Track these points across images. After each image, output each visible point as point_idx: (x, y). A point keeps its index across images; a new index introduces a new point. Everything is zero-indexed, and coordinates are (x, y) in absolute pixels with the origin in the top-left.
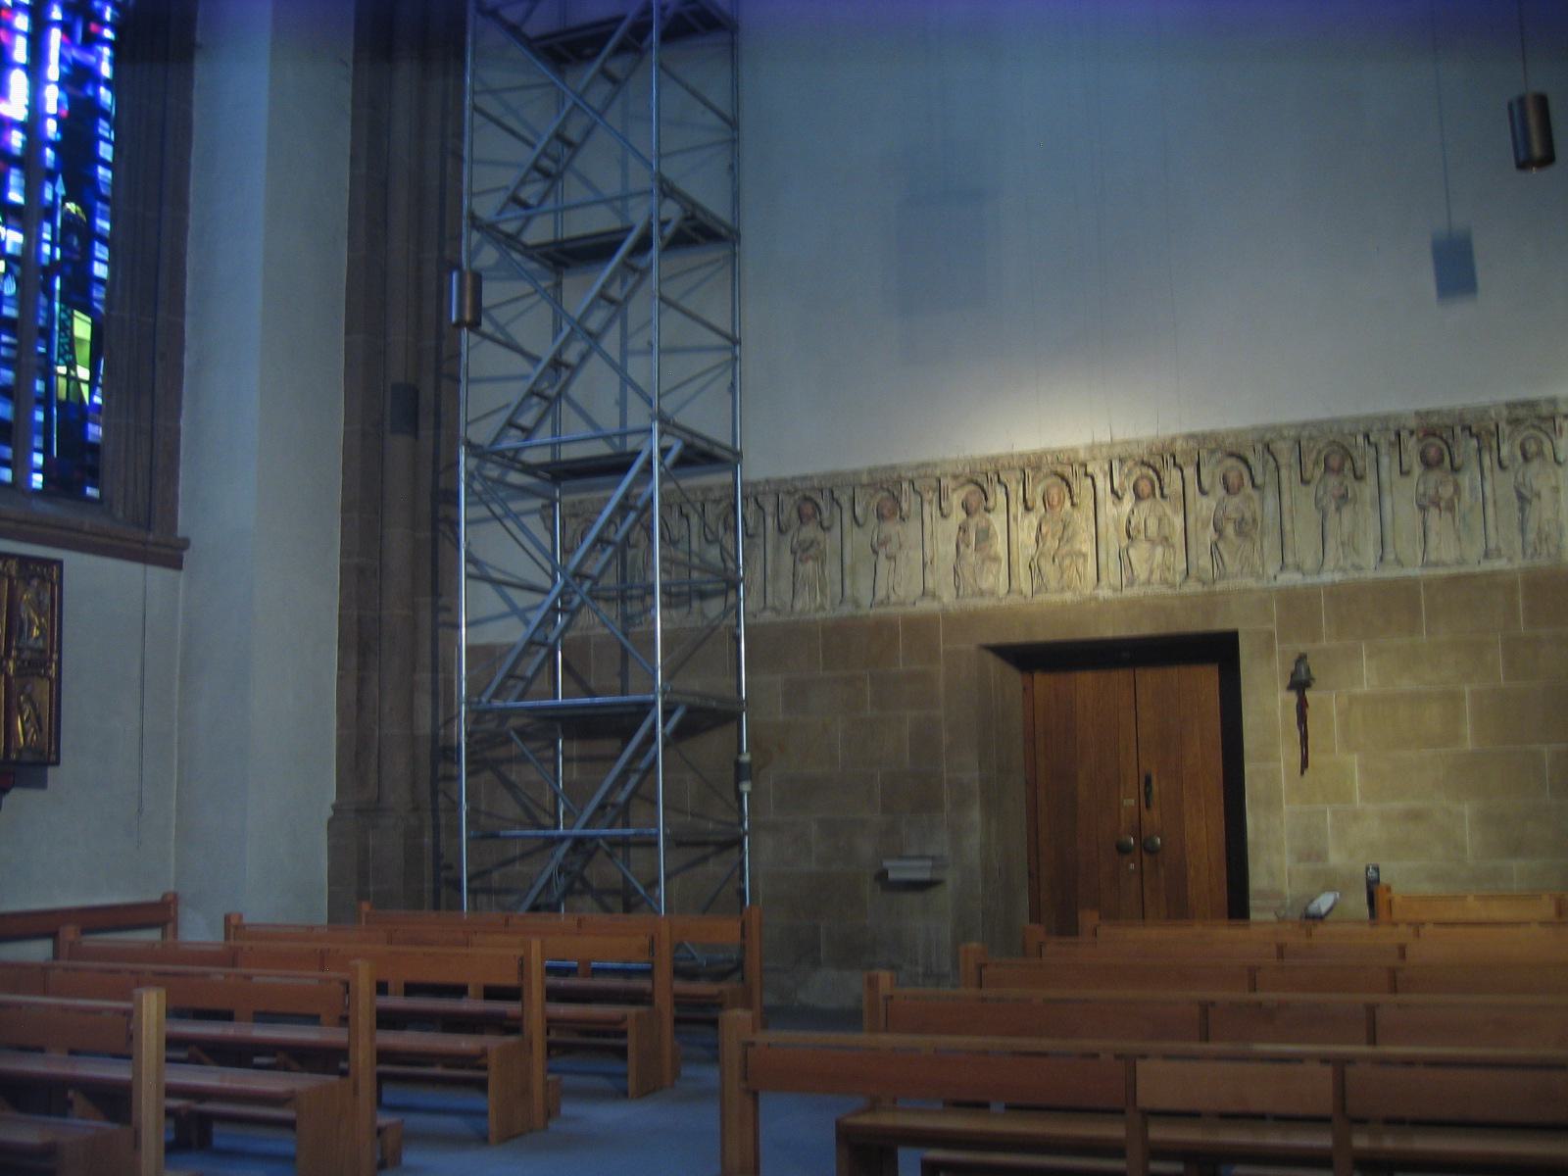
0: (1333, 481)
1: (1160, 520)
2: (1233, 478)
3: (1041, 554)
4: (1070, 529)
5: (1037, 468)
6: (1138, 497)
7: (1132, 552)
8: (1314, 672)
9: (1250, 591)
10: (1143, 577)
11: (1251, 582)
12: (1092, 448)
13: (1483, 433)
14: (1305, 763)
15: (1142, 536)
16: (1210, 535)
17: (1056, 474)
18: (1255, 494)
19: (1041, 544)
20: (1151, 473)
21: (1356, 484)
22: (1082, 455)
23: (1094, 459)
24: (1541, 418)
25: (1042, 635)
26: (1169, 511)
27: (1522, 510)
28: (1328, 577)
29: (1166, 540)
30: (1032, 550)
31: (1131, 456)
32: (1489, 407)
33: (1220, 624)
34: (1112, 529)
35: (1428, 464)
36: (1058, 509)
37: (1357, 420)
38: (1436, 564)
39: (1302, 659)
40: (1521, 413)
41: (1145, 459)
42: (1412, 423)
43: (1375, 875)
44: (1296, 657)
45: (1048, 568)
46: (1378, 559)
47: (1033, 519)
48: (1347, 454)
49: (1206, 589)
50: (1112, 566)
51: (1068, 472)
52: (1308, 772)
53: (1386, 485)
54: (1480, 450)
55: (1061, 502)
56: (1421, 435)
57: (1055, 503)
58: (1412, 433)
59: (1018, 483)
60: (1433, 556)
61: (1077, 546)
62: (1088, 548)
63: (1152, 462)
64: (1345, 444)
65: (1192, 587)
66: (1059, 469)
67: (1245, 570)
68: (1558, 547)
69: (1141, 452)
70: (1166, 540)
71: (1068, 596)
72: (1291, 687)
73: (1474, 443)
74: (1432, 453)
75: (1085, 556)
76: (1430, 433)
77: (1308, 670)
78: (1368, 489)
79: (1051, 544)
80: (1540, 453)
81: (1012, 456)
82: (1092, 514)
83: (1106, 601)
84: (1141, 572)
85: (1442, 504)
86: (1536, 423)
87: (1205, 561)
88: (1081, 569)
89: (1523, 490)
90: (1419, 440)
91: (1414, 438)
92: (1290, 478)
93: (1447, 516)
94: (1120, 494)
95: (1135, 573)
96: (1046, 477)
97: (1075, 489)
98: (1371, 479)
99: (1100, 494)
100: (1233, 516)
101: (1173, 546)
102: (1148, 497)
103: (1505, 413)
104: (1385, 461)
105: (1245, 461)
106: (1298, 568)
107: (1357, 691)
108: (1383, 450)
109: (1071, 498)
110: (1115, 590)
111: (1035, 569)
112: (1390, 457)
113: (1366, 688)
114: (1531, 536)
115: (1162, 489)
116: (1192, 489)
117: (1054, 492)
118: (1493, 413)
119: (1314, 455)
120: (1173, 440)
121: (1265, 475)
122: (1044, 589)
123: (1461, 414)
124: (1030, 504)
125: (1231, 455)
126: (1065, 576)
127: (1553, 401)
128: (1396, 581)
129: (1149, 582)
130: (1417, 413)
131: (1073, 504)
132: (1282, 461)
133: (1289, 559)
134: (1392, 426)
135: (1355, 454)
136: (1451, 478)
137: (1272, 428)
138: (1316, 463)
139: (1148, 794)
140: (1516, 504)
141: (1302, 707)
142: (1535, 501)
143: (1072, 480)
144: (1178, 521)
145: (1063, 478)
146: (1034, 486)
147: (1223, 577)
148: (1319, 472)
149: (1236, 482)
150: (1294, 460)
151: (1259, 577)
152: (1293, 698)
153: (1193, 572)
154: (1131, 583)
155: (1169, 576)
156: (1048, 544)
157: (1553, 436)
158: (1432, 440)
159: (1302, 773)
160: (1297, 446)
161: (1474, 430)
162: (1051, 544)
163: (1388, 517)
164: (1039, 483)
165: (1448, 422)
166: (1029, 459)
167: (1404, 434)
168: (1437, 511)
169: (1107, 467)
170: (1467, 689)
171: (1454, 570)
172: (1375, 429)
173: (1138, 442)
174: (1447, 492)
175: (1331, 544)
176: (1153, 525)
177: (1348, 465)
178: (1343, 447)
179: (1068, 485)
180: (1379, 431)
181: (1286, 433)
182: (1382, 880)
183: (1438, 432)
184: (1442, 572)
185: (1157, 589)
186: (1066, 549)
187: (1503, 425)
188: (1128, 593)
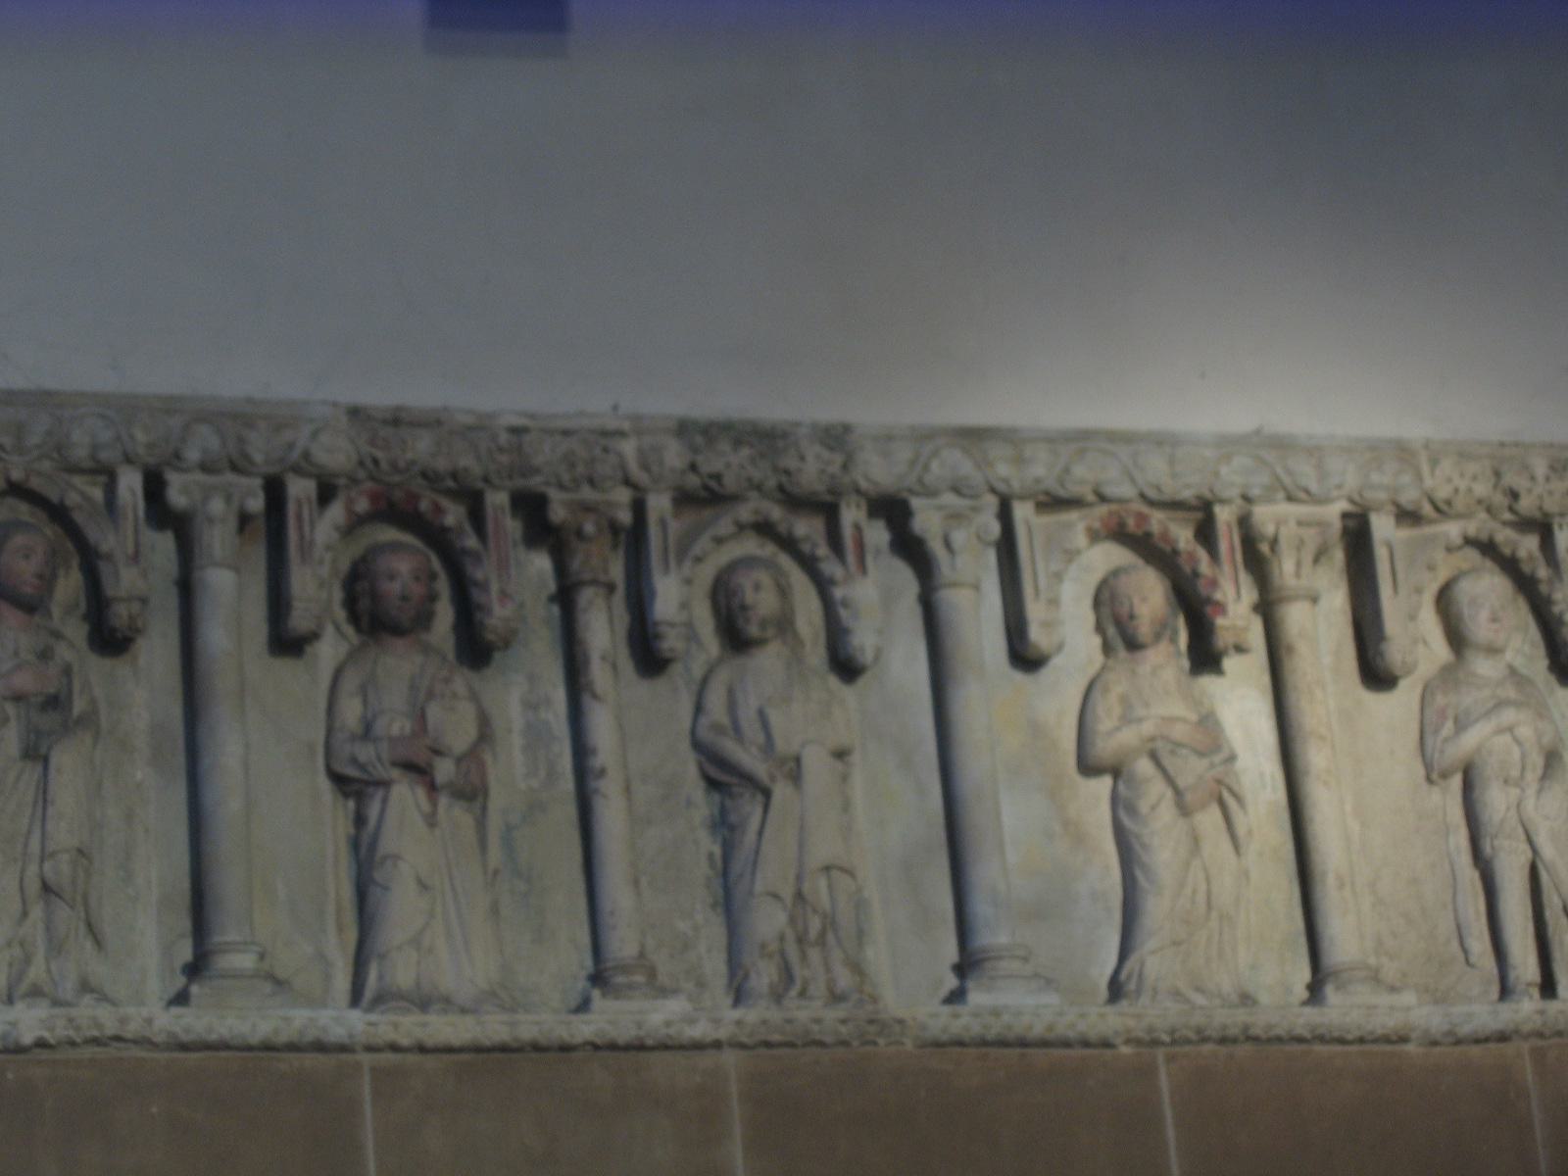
13: (589, 528)
21: (96, 669)
24: (796, 502)
27: (725, 827)
32: (621, 434)
37: (124, 408)
38: (423, 1001)
40: (730, 463)
42: (336, 452)
53: (221, 680)
54: (565, 596)
56: (362, 505)
58: (326, 494)
60: (403, 973)
64: (72, 499)
68: (857, 968)
73: (541, 563)
74: (403, 566)
80: (784, 624)
85: (444, 770)
86: (776, 513)
89: (730, 748)
90: (354, 525)
91: (336, 512)
93: (456, 816)
98: (157, 650)
103: (674, 456)
108: (217, 538)
114: (768, 921)
118: (628, 448)
123: (516, 431)
127: (836, 437)
128: (268, 1047)
130: (355, 413)
134: (260, 449)
135: (105, 539)
136: (459, 685)
140: (701, 805)
142: (781, 791)
157: (830, 568)
158: (389, 534)
161: (558, 513)
165: (466, 461)
167: (300, 489)
168: (421, 793)
171: (494, 1028)
172: (193, 455)
177: (70, 585)
178: (58, 514)
187: (659, 504)
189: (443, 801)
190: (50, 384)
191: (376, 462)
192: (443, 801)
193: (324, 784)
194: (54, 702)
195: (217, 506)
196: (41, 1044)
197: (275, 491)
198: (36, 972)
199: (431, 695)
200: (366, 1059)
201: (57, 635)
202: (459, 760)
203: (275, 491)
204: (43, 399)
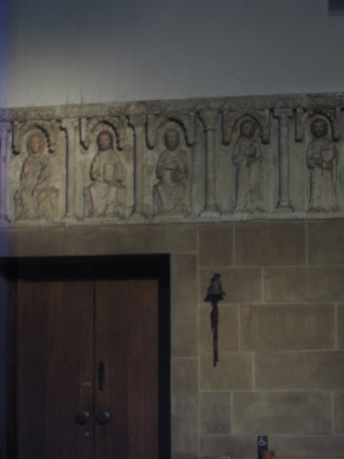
0: (246, 143)
1: (115, 166)
2: (172, 138)
3: (23, 189)
4: (47, 169)
5: (24, 121)
6: (101, 148)
7: (93, 190)
8: (225, 288)
9: (181, 224)
10: (100, 209)
11: (181, 218)
12: (66, 107)
14: (216, 359)
15: (101, 179)
16: (153, 180)
17: (39, 127)
18: (187, 150)
19: (24, 181)
20: (110, 130)
21: (263, 146)
22: (58, 113)
23: (67, 117)
25: (22, 252)
26: (123, 160)
28: (237, 216)
29: (119, 182)
30: (17, 185)
31: (96, 116)
33: (156, 249)
34: (79, 172)
35: (316, 135)
36: (37, 155)
37: (264, 98)
38: (318, 210)
39: (216, 277)
41: (107, 118)
42: (305, 103)
43: (264, 444)
44: (212, 276)
45: (27, 198)
46: (276, 205)
47: (19, 160)
48: (256, 123)
49: (147, 221)
50: (79, 199)
51: (47, 125)
52: (218, 364)
55: (41, 149)
56: (311, 113)
57: (36, 149)
58: (305, 110)
59: (9, 131)
60: (316, 205)
61: (52, 184)
62: (60, 185)
63: (111, 121)
64: (256, 116)
65: (138, 219)
66: (40, 123)
67: (177, 208)
69: (103, 112)
70: (119, 182)
71: (43, 222)
72: (207, 300)
74: (319, 124)
75: (57, 191)
76: (317, 112)
77: (220, 287)
78: (271, 152)
79: (32, 181)
81: (4, 110)
82: (64, 159)
83: (71, 227)
84: (99, 206)
85: (324, 165)
87: (148, 200)
88: (54, 201)
90: (310, 116)
91: (306, 115)
92: (214, 140)
93: (328, 174)
94: (86, 144)
95: (95, 208)
96: (31, 128)
97: (52, 140)
99: (71, 145)
100: (170, 166)
101: (124, 187)
102: (107, 148)
104: (284, 130)
105: (181, 124)
106: (217, 208)
107: (256, 303)
108: (284, 121)
109: (49, 146)
110: (79, 219)
111: (18, 200)
112: (289, 129)
113: (263, 302)
115: (118, 142)
116: (141, 144)
117: (36, 140)
119: (232, 123)
120: (128, 105)
121: (195, 135)
122: (24, 216)
124: (16, 149)
125: (171, 119)
126: (41, 207)
128: (288, 220)
129: (104, 214)
130: (309, 95)
131: (51, 152)
132: (209, 127)
133: (211, 202)
135: (262, 124)
136: (331, 146)
137: (202, 100)
138: (234, 128)
139: (101, 378)
141: (214, 316)
143: (50, 132)
144: (129, 168)
145: (44, 131)
146: (22, 135)
147: (161, 212)
148: (236, 135)
149: (174, 139)
150: (217, 127)
151: (188, 214)
152: (209, 306)
153: (138, 208)
154: (91, 214)
155: (120, 209)
156: (29, 181)
159: (215, 365)
160: (220, 115)
162: (32, 181)
163: (285, 173)
164: (26, 131)
166: (17, 113)
167: (299, 110)
168: (320, 169)
169: (77, 124)
170: (336, 304)
171: (330, 215)
172: (278, 106)
173: (101, 105)
174: (328, 156)
175: (243, 191)
176: (110, 169)
178: (254, 119)
179: (47, 136)
180: (281, 108)
181: (212, 105)
182: (270, 448)
183: (323, 112)
184: (321, 216)
185: (111, 219)
186: (40, 187)
188: (89, 221)
189: (325, 171)
190: (251, 94)
191: (313, 105)
192: (325, 171)
193: (306, 167)
194: (252, 156)
195: (283, 115)
196: (247, 220)
197: (295, 110)
198: (249, 206)
199: (324, 150)
200: (307, 221)
201: (255, 141)
202: (327, 163)
203: (295, 110)
204: (250, 97)
